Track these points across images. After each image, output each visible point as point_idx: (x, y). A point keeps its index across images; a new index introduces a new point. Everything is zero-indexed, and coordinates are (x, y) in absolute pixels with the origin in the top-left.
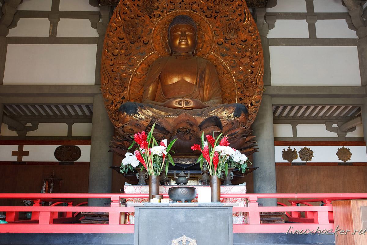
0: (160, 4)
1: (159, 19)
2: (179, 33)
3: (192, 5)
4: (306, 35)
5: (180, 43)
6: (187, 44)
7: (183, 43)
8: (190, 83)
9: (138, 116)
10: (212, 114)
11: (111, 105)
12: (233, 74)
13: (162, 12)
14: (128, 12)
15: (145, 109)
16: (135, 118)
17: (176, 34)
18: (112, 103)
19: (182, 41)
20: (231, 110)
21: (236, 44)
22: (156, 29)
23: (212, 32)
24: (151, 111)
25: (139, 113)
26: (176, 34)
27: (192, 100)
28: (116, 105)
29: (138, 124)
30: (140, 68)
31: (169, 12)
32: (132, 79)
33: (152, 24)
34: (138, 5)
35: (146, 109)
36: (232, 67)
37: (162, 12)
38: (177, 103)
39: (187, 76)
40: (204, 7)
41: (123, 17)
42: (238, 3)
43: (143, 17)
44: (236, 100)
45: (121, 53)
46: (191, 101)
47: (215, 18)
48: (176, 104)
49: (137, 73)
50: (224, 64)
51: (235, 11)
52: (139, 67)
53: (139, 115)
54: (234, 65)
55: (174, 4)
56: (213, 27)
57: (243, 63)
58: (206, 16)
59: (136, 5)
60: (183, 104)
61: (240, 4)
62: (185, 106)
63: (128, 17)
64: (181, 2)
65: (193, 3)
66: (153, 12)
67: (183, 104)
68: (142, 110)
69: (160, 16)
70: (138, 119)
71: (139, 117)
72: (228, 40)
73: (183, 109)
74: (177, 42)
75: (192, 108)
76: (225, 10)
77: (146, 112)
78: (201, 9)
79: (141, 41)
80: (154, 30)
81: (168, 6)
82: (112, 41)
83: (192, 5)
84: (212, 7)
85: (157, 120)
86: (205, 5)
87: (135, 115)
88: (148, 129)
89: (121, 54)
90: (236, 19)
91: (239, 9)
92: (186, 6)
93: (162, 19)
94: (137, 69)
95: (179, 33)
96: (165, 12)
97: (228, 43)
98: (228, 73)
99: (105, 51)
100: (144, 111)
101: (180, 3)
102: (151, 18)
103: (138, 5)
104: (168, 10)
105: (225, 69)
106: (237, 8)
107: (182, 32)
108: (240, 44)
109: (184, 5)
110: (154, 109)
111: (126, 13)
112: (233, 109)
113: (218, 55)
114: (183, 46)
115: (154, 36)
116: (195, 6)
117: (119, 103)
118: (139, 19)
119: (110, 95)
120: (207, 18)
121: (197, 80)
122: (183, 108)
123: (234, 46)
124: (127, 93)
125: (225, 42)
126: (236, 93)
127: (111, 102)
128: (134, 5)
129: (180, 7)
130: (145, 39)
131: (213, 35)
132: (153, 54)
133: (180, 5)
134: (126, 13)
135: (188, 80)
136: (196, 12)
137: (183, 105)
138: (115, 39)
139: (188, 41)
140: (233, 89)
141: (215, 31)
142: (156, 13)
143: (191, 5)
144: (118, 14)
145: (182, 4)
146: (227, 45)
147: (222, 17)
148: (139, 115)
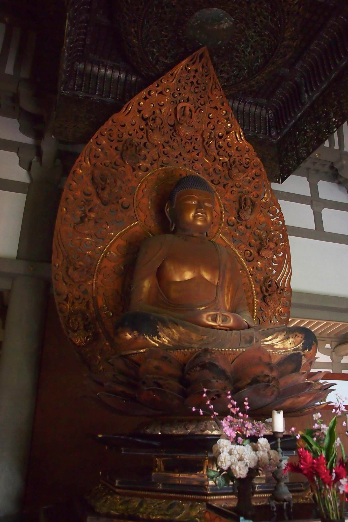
0: (148, 152)
1: (147, 174)
2: (194, 202)
3: (193, 162)
4: (312, 226)
5: (195, 217)
6: (205, 220)
7: (200, 218)
8: (210, 282)
9: (158, 339)
10: (267, 343)
11: (65, 302)
12: (250, 271)
13: (152, 164)
14: (102, 155)
15: (168, 327)
16: (153, 342)
17: (189, 202)
18: (67, 300)
19: (199, 216)
20: (299, 339)
21: (252, 227)
22: (142, 188)
23: (220, 205)
24: (177, 331)
25: (160, 333)
26: (189, 202)
27: (233, 316)
28: (73, 303)
29: (166, 358)
30: (116, 245)
31: (162, 166)
32: (101, 261)
33: (135, 179)
34: (116, 149)
35: (170, 327)
36: (248, 261)
37: (152, 164)
38: (210, 318)
39: (206, 271)
40: (210, 169)
41: (94, 161)
42: (255, 171)
43: (124, 167)
44: (254, 311)
45: (90, 217)
46: (230, 316)
47: (224, 186)
48: (209, 321)
49: (110, 253)
50: (237, 255)
51: (250, 182)
52: (113, 242)
53: (159, 337)
54: (250, 258)
55: (169, 157)
56: (221, 198)
57: (263, 257)
58: (212, 182)
59: (114, 147)
60: (220, 321)
61: (258, 174)
62: (221, 325)
63: (101, 164)
64: (179, 156)
65: (194, 159)
66: (139, 163)
67: (220, 321)
68: (164, 328)
69: (147, 170)
70: (157, 345)
71: (159, 341)
72: (242, 220)
73: (217, 329)
74: (192, 215)
75: (231, 329)
76: (239, 178)
77: (170, 332)
78: (206, 170)
79: (118, 202)
80: (139, 189)
81: (159, 157)
82: (73, 196)
83: (193, 162)
84: (220, 170)
85: (211, 355)
86: (211, 165)
87: (152, 337)
88: (193, 371)
89: (90, 218)
90: (252, 192)
91: (256, 180)
92: (186, 162)
93: (151, 175)
94: (111, 246)
95: (194, 202)
96: (155, 166)
97: (241, 225)
98: (243, 268)
99: (62, 210)
100: (166, 330)
101: (177, 157)
102: (134, 170)
103: (116, 149)
104: (160, 163)
105: (239, 263)
106: (254, 179)
107: (199, 202)
108: (257, 229)
109: (182, 160)
110: (181, 328)
111: (98, 157)
112: (302, 337)
113: (230, 240)
114: (199, 223)
115: (139, 198)
116: (198, 165)
117: (77, 299)
118: (117, 170)
119: (64, 284)
120: (213, 185)
121: (219, 279)
122: (218, 327)
123: (249, 231)
124: (92, 284)
125: (238, 223)
126: (253, 301)
127: (65, 297)
128: (111, 147)
129: (177, 162)
130: (125, 200)
131: (221, 211)
132: (136, 225)
133: (176, 159)
134: (98, 157)
135: (207, 276)
136: (200, 174)
137: (219, 323)
138: (78, 193)
139: (207, 216)
140: (250, 294)
141: (224, 204)
142: (143, 164)
143: (191, 162)
144: (87, 155)
145: (180, 159)
146: (240, 227)
147: (232, 187)
148: (159, 337)
